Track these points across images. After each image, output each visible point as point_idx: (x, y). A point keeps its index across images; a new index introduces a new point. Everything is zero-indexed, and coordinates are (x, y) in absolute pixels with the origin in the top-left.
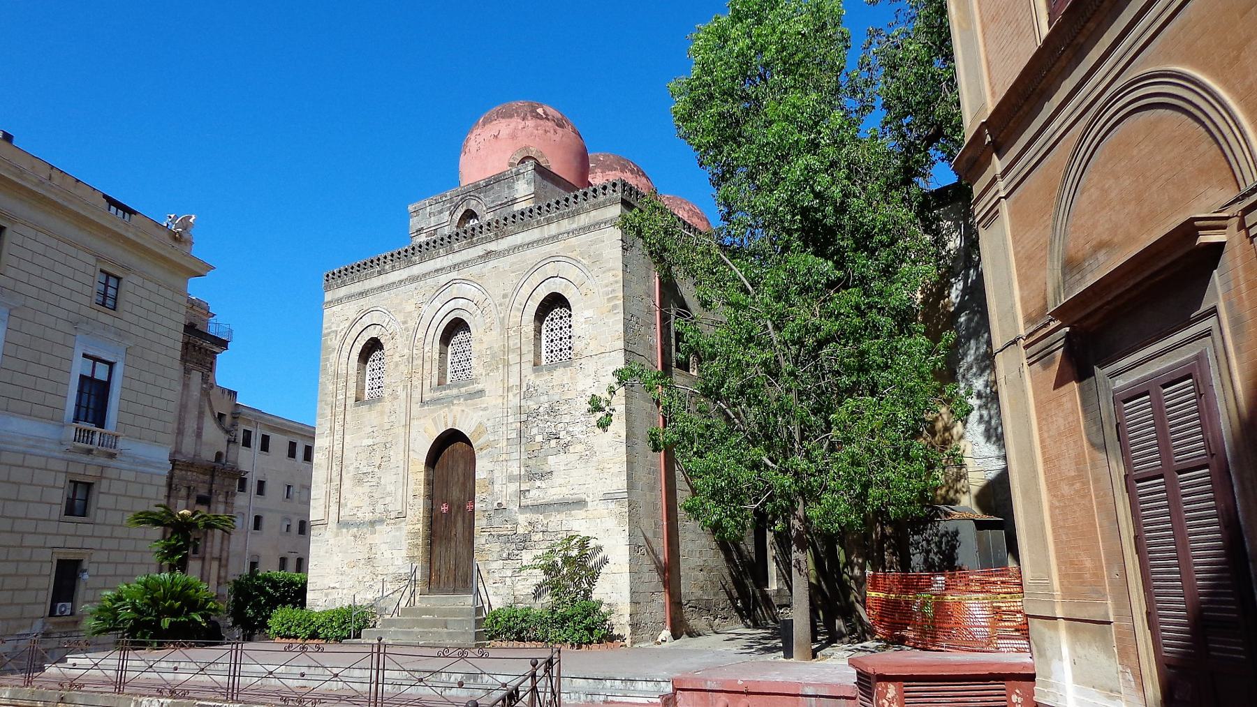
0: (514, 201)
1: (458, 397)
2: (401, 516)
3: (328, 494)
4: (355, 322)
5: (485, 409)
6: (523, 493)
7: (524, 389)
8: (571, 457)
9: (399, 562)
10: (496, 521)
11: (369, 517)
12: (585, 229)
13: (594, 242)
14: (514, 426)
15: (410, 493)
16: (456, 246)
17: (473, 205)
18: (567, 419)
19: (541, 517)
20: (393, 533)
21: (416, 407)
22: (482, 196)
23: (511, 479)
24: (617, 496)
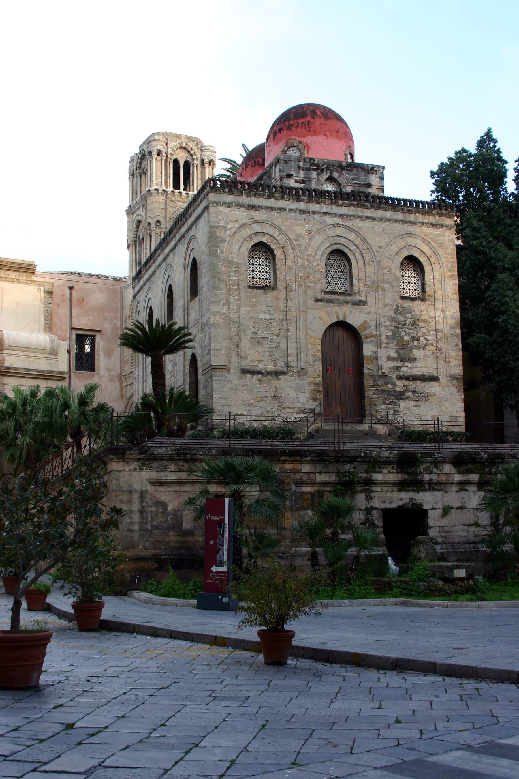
0: (369, 186)
1: (347, 302)
2: (302, 372)
3: (229, 348)
4: (243, 225)
5: (368, 314)
6: (398, 368)
7: (395, 307)
8: (427, 353)
9: (304, 401)
10: (381, 382)
11: (270, 368)
12: (435, 225)
13: (438, 235)
14: (390, 328)
15: (310, 356)
16: (340, 202)
17: (336, 175)
18: (424, 330)
19: (411, 383)
20: (297, 381)
21: (311, 302)
22: (344, 172)
23: (390, 358)
24: (457, 376)
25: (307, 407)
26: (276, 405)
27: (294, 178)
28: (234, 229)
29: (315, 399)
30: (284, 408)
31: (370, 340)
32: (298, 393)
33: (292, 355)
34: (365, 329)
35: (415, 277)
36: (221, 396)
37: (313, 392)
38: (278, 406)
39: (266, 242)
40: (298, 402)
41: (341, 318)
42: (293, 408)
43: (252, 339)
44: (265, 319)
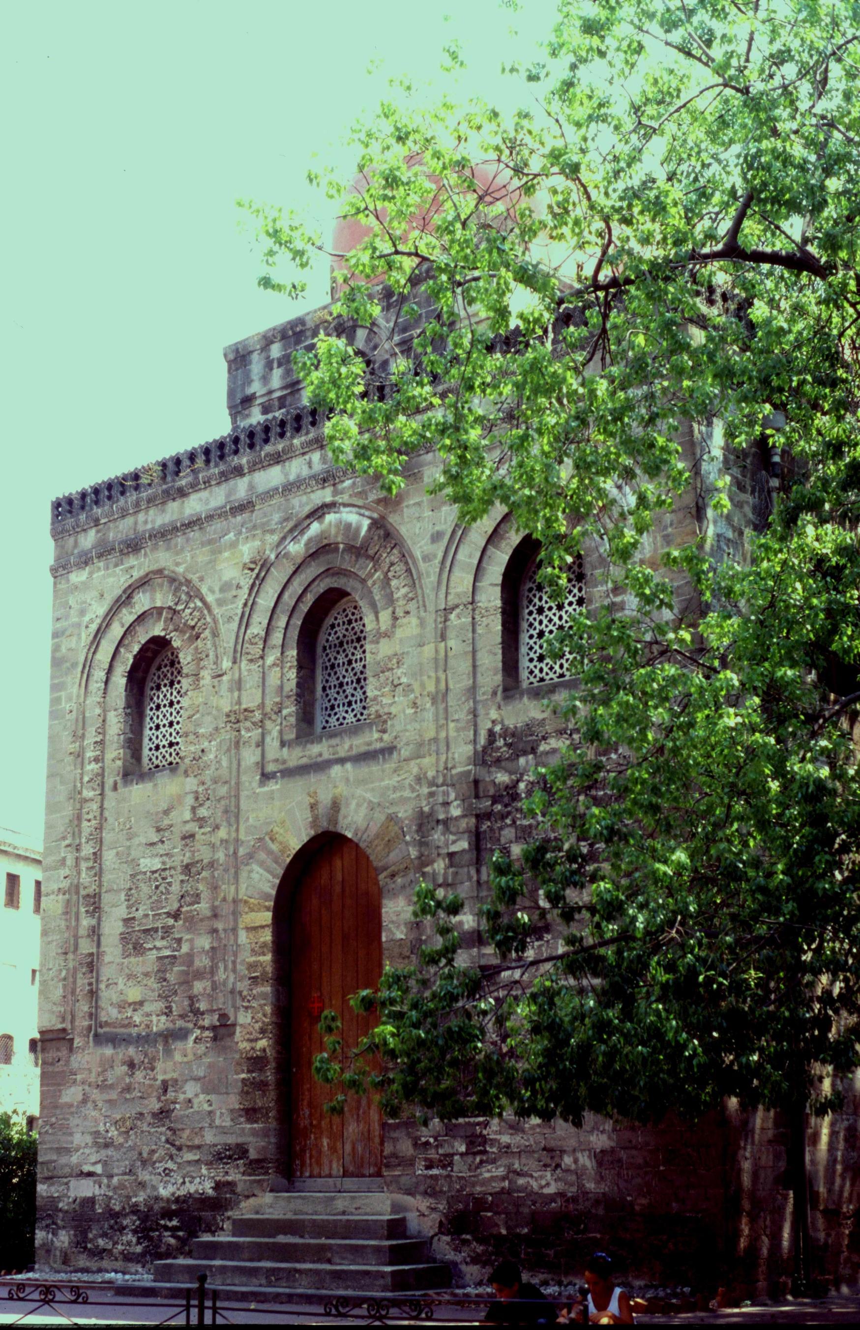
7: (482, 740)
25: (232, 1140)
26: (163, 1139)
27: (259, 401)
28: (94, 627)
29: (251, 1113)
30: (179, 1149)
31: (399, 880)
32: (212, 1097)
33: (199, 975)
34: (389, 844)
35: (541, 611)
36: (53, 1120)
37: (251, 1087)
38: (167, 1141)
39: (162, 634)
40: (211, 1126)
41: (324, 825)
42: (199, 1147)
43: (124, 938)
44: (153, 872)
